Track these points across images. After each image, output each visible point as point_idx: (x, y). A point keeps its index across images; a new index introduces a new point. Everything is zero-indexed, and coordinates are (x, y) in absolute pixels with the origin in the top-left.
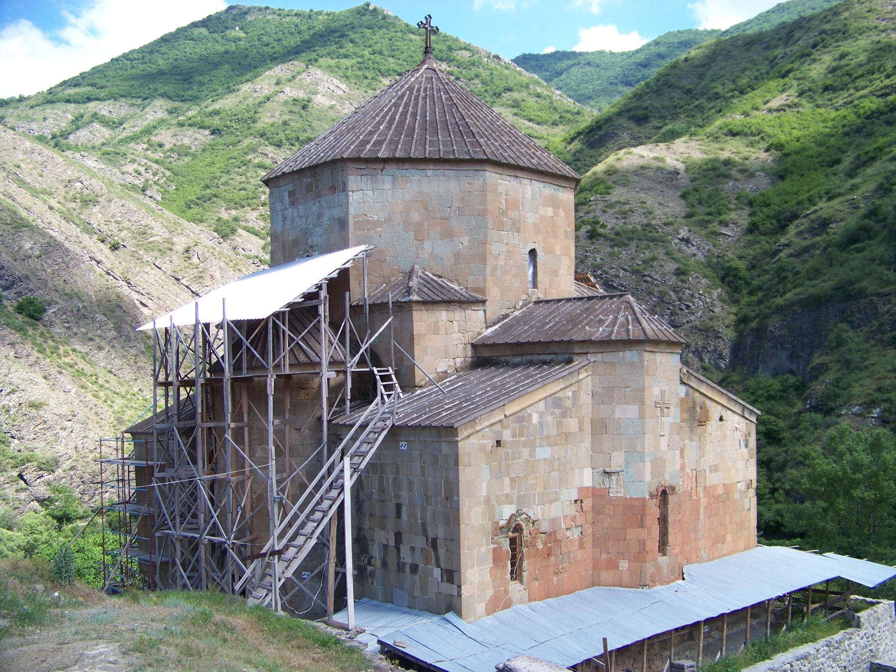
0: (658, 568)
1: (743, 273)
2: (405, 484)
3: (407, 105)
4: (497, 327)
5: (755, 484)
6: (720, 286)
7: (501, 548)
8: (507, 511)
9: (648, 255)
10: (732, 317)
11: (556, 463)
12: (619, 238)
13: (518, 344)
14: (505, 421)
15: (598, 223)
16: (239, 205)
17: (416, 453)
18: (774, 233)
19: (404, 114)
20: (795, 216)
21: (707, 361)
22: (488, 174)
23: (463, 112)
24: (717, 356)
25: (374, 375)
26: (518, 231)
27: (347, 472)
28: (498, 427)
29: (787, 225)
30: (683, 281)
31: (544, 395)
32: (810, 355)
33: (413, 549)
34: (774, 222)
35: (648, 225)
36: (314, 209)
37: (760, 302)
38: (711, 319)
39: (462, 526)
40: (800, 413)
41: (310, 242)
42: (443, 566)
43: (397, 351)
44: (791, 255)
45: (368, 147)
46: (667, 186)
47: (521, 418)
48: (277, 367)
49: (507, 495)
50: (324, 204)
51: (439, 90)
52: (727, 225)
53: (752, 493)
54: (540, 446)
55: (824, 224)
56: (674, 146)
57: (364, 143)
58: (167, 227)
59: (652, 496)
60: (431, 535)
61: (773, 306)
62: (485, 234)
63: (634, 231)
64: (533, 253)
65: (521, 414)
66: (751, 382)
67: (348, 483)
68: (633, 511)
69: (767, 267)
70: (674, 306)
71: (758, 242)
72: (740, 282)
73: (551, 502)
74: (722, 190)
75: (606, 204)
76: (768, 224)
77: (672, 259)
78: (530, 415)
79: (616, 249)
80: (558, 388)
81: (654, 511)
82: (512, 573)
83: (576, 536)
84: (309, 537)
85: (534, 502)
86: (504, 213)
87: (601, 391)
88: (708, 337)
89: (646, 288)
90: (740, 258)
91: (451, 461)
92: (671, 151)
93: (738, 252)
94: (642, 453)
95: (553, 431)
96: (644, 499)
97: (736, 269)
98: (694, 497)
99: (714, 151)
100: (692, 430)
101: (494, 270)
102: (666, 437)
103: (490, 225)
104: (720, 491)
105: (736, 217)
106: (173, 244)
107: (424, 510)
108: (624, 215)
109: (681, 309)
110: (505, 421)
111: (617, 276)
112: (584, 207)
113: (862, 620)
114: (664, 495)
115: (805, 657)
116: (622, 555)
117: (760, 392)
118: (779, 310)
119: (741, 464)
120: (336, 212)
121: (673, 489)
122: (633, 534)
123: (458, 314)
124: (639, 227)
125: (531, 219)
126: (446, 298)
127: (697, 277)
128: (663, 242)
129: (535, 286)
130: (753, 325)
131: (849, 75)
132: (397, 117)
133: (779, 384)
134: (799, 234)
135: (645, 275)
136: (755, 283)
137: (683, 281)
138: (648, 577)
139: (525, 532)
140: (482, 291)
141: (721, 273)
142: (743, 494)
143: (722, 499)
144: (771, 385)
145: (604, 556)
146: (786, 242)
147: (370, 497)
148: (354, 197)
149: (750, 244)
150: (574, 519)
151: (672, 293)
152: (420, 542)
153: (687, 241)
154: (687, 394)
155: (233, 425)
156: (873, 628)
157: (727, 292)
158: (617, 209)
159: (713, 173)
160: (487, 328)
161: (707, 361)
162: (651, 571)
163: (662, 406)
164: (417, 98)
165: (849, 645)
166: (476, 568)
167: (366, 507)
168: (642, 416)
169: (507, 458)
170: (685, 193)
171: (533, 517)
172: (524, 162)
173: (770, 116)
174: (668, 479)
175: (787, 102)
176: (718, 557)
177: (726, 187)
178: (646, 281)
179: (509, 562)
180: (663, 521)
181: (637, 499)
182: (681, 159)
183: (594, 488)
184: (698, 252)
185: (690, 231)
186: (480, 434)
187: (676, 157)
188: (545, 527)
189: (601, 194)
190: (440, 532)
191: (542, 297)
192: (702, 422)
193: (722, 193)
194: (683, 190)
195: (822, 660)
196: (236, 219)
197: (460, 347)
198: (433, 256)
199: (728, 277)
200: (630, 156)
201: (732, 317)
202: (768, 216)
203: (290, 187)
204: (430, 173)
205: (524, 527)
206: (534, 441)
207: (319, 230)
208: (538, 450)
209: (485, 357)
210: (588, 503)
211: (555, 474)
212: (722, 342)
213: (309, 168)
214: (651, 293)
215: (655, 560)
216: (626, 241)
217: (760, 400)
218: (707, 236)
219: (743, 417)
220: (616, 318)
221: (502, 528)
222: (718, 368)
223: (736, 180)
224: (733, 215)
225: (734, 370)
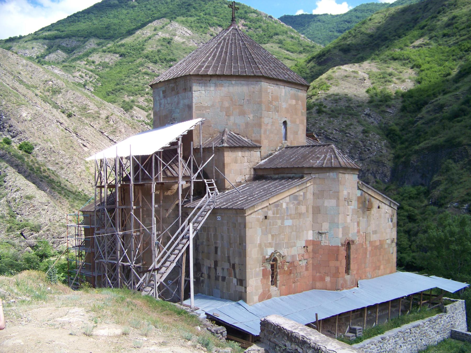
0: (345, 281)
1: (398, 132)
3: (222, 48)
4: (266, 160)
5: (395, 241)
6: (386, 139)
7: (266, 269)
8: (270, 251)
9: (348, 122)
10: (392, 155)
12: (333, 113)
13: (277, 169)
14: (269, 206)
15: (322, 105)
16: (134, 94)
17: (225, 222)
18: (414, 111)
19: (221, 52)
20: (426, 103)
21: (378, 178)
22: (263, 83)
23: (251, 51)
25: (205, 183)
26: (278, 112)
28: (266, 209)
29: (422, 108)
30: (366, 136)
31: (289, 194)
32: (432, 176)
34: (415, 106)
35: (349, 107)
36: (176, 99)
37: (407, 148)
38: (380, 156)
39: (247, 258)
40: (426, 206)
41: (173, 116)
42: (238, 277)
43: (216, 171)
44: (423, 123)
45: (203, 69)
46: (359, 86)
47: (277, 205)
48: (157, 179)
49: (270, 243)
50: (180, 97)
51: (239, 40)
52: (390, 107)
53: (394, 245)
54: (287, 219)
55: (441, 107)
56: (363, 65)
57: (201, 67)
58: (97, 105)
59: (342, 245)
60: (232, 262)
61: (413, 150)
63: (341, 110)
64: (285, 123)
65: (277, 203)
66: (401, 190)
67: (192, 236)
68: (333, 252)
69: (410, 129)
70: (361, 149)
71: (406, 117)
72: (397, 137)
73: (292, 247)
74: (388, 89)
76: (411, 106)
78: (282, 204)
79: (332, 119)
80: (296, 191)
81: (343, 252)
83: (304, 264)
84: (172, 263)
85: (283, 246)
87: (318, 192)
88: (379, 165)
89: (347, 140)
90: (397, 124)
91: (242, 226)
92: (361, 68)
94: (338, 224)
95: (293, 212)
96: (338, 246)
97: (394, 130)
98: (364, 246)
100: (364, 213)
101: (265, 131)
102: (350, 216)
103: (264, 109)
104: (378, 243)
105: (395, 103)
107: (228, 250)
109: (365, 151)
110: (269, 206)
111: (332, 133)
113: (447, 309)
114: (348, 245)
115: (418, 326)
117: (406, 195)
118: (416, 152)
119: (388, 230)
120: (186, 101)
121: (353, 241)
122: (333, 264)
123: (247, 154)
124: (344, 108)
125: (284, 105)
126: (241, 145)
128: (356, 116)
129: (286, 139)
130: (403, 160)
131: (457, 28)
132: (217, 54)
133: (415, 191)
134: (428, 112)
135: (347, 133)
136: (404, 138)
137: (366, 136)
138: (340, 285)
139: (279, 262)
140: (259, 142)
142: (390, 245)
143: (379, 248)
144: (411, 191)
145: (318, 274)
146: (421, 116)
147: (202, 243)
148: (195, 94)
149: (401, 117)
150: (303, 256)
151: (360, 143)
152: (226, 266)
153: (368, 115)
154: (361, 195)
155: (134, 207)
156: (453, 313)
157: (389, 142)
159: (383, 80)
160: (261, 160)
161: (378, 178)
163: (348, 200)
164: (227, 44)
165: (440, 321)
166: (254, 279)
167: (200, 248)
168: (338, 205)
169: (270, 225)
170: (368, 90)
171: (282, 254)
172: (281, 77)
173: (414, 50)
174: (351, 237)
175: (423, 43)
177: (390, 87)
178: (347, 136)
179: (270, 276)
180: (348, 258)
181: (335, 246)
182: (367, 72)
183: (313, 241)
185: (370, 110)
186: (257, 213)
187: (364, 71)
188: (288, 259)
189: (324, 90)
190: (237, 261)
191: (289, 145)
193: (387, 90)
194: (367, 88)
195: (426, 328)
196: (133, 101)
197: (248, 169)
199: (390, 134)
201: (392, 155)
202: (412, 103)
203: (163, 89)
204: (233, 82)
206: (284, 216)
207: (178, 110)
208: (285, 221)
209: (260, 175)
210: (310, 248)
211: (294, 233)
212: (386, 169)
213: (173, 79)
214: (349, 142)
215: (343, 277)
216: (337, 115)
217: (405, 199)
219: (390, 206)
220: (326, 156)
221: (267, 259)
222: (384, 182)
223: (395, 83)
225: (392, 183)
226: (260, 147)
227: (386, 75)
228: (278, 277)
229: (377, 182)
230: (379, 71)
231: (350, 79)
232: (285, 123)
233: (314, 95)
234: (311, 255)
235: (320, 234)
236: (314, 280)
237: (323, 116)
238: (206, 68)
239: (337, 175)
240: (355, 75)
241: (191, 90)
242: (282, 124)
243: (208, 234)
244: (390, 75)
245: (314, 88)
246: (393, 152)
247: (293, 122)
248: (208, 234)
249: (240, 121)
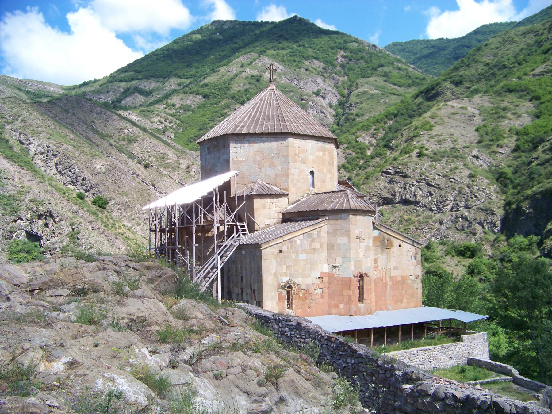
0: (359, 309)
1: (510, 175)
4: (294, 205)
5: (421, 277)
9: (453, 166)
10: (503, 202)
14: (284, 242)
15: (424, 147)
18: (530, 151)
19: (256, 112)
20: (542, 141)
21: (486, 228)
22: (289, 139)
23: (282, 110)
24: (492, 225)
26: (305, 163)
27: (219, 262)
28: (280, 244)
29: (537, 146)
30: (473, 181)
32: (546, 224)
33: (247, 294)
34: (530, 144)
35: (453, 148)
36: (217, 155)
37: (519, 193)
38: (489, 203)
39: (263, 284)
40: (538, 257)
42: (257, 300)
44: (539, 164)
45: (238, 128)
46: (468, 124)
48: (197, 222)
49: (285, 273)
52: (502, 147)
53: (419, 281)
56: (473, 100)
58: (176, 154)
59: (354, 277)
60: (253, 288)
61: (525, 195)
62: (288, 165)
63: (445, 152)
64: (312, 173)
66: (512, 241)
67: (220, 267)
68: (346, 283)
69: (524, 172)
70: (467, 196)
71: (520, 157)
72: (509, 181)
73: (307, 277)
74: (501, 126)
75: (429, 136)
76: (526, 146)
77: (467, 168)
78: (296, 241)
79: (434, 163)
82: (287, 305)
83: (319, 293)
86: (298, 155)
88: (487, 214)
89: (452, 186)
90: (509, 166)
92: (471, 103)
93: (508, 163)
95: (307, 248)
96: (350, 278)
97: (506, 173)
98: (384, 281)
99: (498, 102)
100: (382, 250)
102: (363, 252)
103: (290, 161)
104: (399, 279)
106: (180, 164)
107: (250, 278)
108: (440, 142)
109: (472, 198)
111: (434, 179)
112: (417, 138)
113: (464, 338)
114: (361, 277)
115: (427, 350)
116: (341, 302)
117: (517, 246)
119: (412, 267)
121: (366, 274)
122: (346, 293)
123: (275, 200)
124: (448, 150)
125: (311, 157)
126: (269, 193)
127: (482, 179)
128: (462, 158)
130: (514, 206)
133: (527, 241)
134: (544, 151)
136: (517, 181)
139: (294, 289)
140: (287, 190)
141: (497, 176)
144: (523, 242)
145: (333, 302)
146: (536, 156)
148: (232, 150)
149: (515, 158)
150: (318, 285)
151: (466, 188)
152: (249, 291)
153: (477, 157)
155: (180, 246)
156: (471, 343)
157: (499, 187)
158: (436, 139)
161: (486, 228)
162: (354, 309)
163: (360, 238)
164: (263, 104)
165: (455, 348)
167: (231, 279)
168: (349, 242)
170: (478, 128)
171: (297, 282)
172: (308, 132)
173: (534, 79)
174: (363, 270)
175: (545, 70)
176: (398, 309)
177: (503, 124)
178: (451, 182)
179: (286, 301)
180: (361, 288)
182: (477, 108)
183: (328, 273)
184: (484, 163)
185: (479, 151)
187: (475, 106)
188: (303, 287)
189: (427, 130)
190: (256, 286)
193: (500, 127)
194: (477, 126)
197: (276, 214)
199: (500, 178)
200: (446, 107)
202: (526, 141)
203: (208, 146)
204: (264, 139)
205: (293, 286)
208: (300, 255)
209: (287, 218)
210: (325, 279)
211: (309, 266)
212: (496, 217)
214: (454, 189)
216: (440, 158)
217: (516, 250)
218: (489, 154)
220: (339, 200)
221: (282, 286)
222: (493, 232)
223: (510, 119)
224: (506, 141)
225: (502, 233)
226: (287, 195)
227: (500, 110)
228: (294, 302)
229: (485, 233)
230: (492, 105)
231: (457, 117)
232: (312, 173)
233: (416, 136)
234: (327, 285)
235: (334, 267)
236: (330, 307)
237: (424, 160)
238: (241, 127)
239: (348, 216)
240: (464, 111)
241: (228, 147)
242: (309, 174)
243: (236, 267)
244: (504, 109)
245: (416, 129)
246: (504, 198)
248: (236, 267)
249: (271, 172)
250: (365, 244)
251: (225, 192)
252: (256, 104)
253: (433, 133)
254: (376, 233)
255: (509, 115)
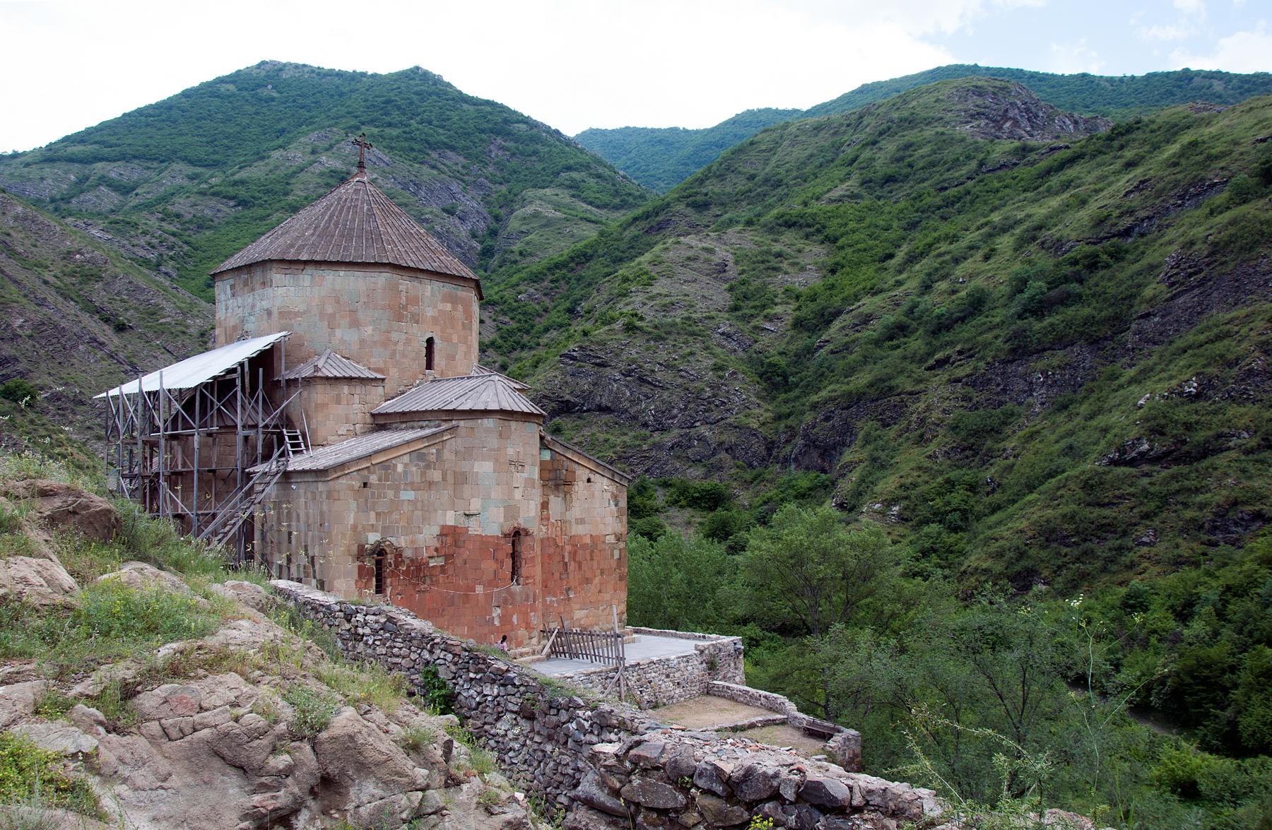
2: (294, 515)
8: (373, 538)
11: (419, 504)
13: (404, 413)
17: (302, 491)
20: (838, 313)
26: (417, 322)
28: (366, 472)
33: (298, 566)
35: (689, 318)
44: (832, 352)
52: (771, 320)
55: (867, 319)
60: (311, 554)
78: (395, 466)
86: (405, 308)
95: (417, 479)
107: (306, 535)
108: (666, 308)
118: (814, 407)
119: (610, 520)
123: (359, 389)
125: (430, 312)
131: (910, 166)
150: (436, 550)
174: (522, 522)
180: (514, 556)
192: (569, 483)
198: (342, 341)
204: (342, 273)
223: (786, 273)
244: (779, 255)
247: (447, 340)
250: (525, 475)
251: (261, 370)
252: (328, 209)
253: (655, 290)
254: (547, 455)
255: (785, 265)
